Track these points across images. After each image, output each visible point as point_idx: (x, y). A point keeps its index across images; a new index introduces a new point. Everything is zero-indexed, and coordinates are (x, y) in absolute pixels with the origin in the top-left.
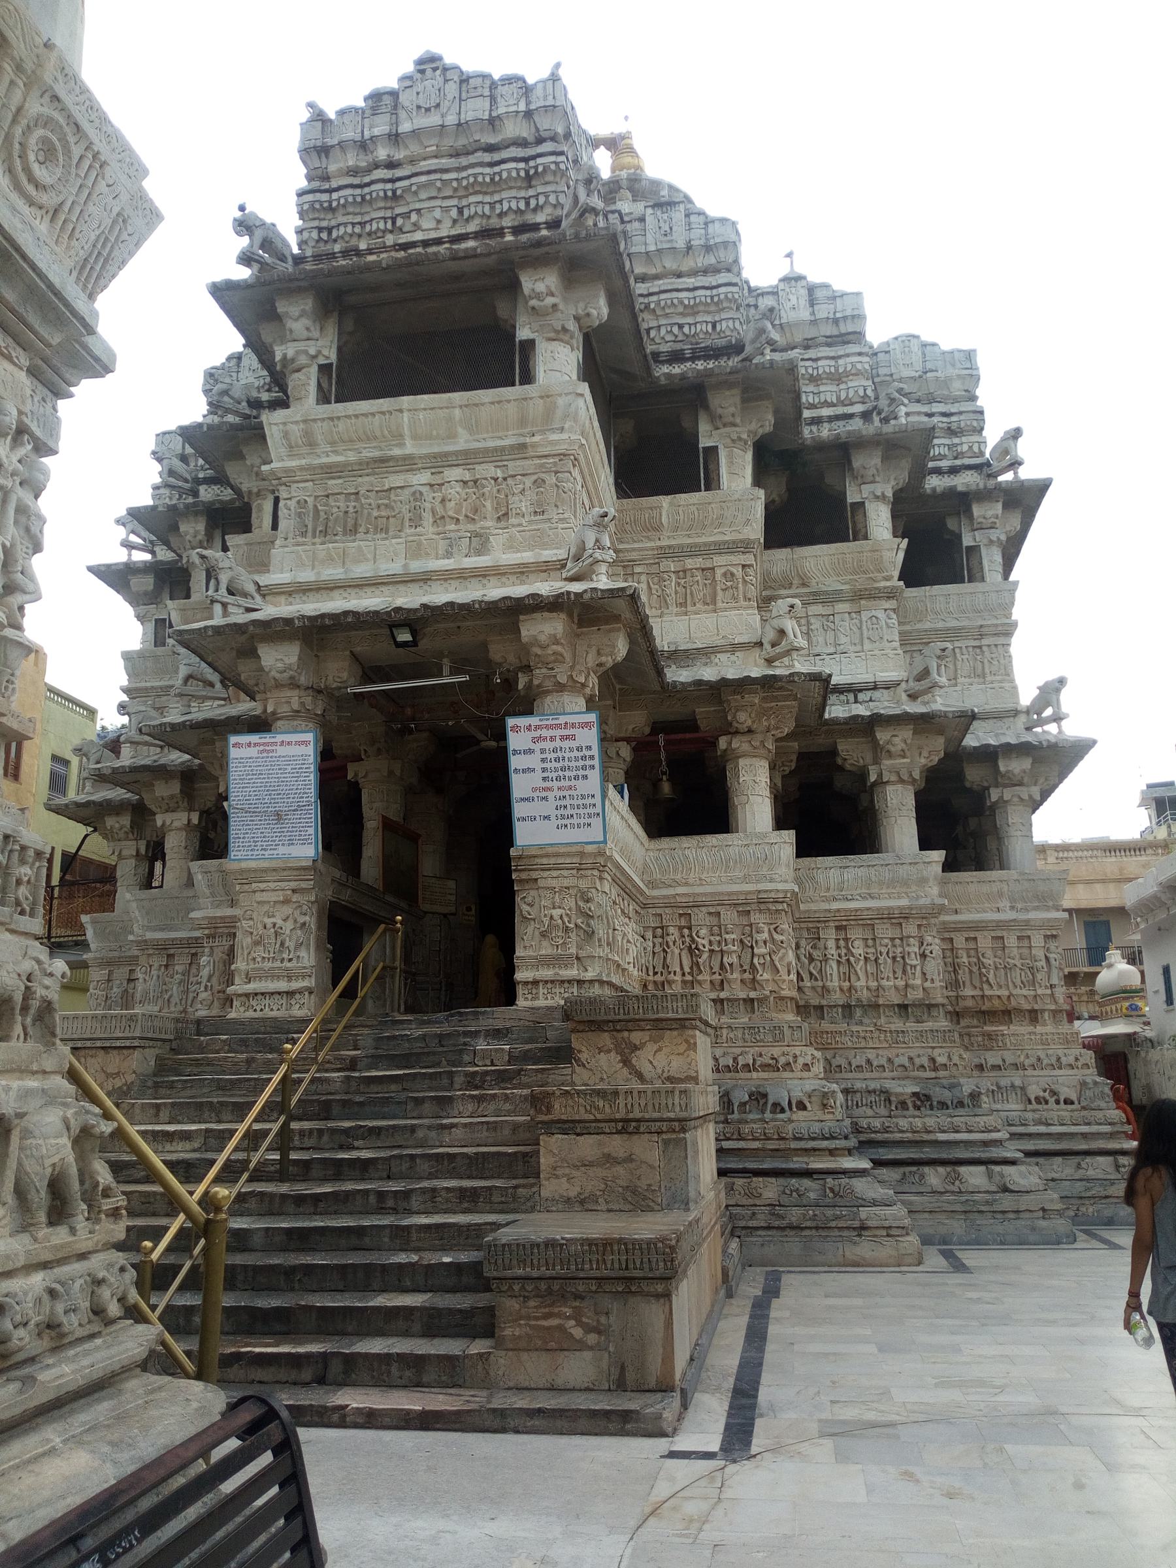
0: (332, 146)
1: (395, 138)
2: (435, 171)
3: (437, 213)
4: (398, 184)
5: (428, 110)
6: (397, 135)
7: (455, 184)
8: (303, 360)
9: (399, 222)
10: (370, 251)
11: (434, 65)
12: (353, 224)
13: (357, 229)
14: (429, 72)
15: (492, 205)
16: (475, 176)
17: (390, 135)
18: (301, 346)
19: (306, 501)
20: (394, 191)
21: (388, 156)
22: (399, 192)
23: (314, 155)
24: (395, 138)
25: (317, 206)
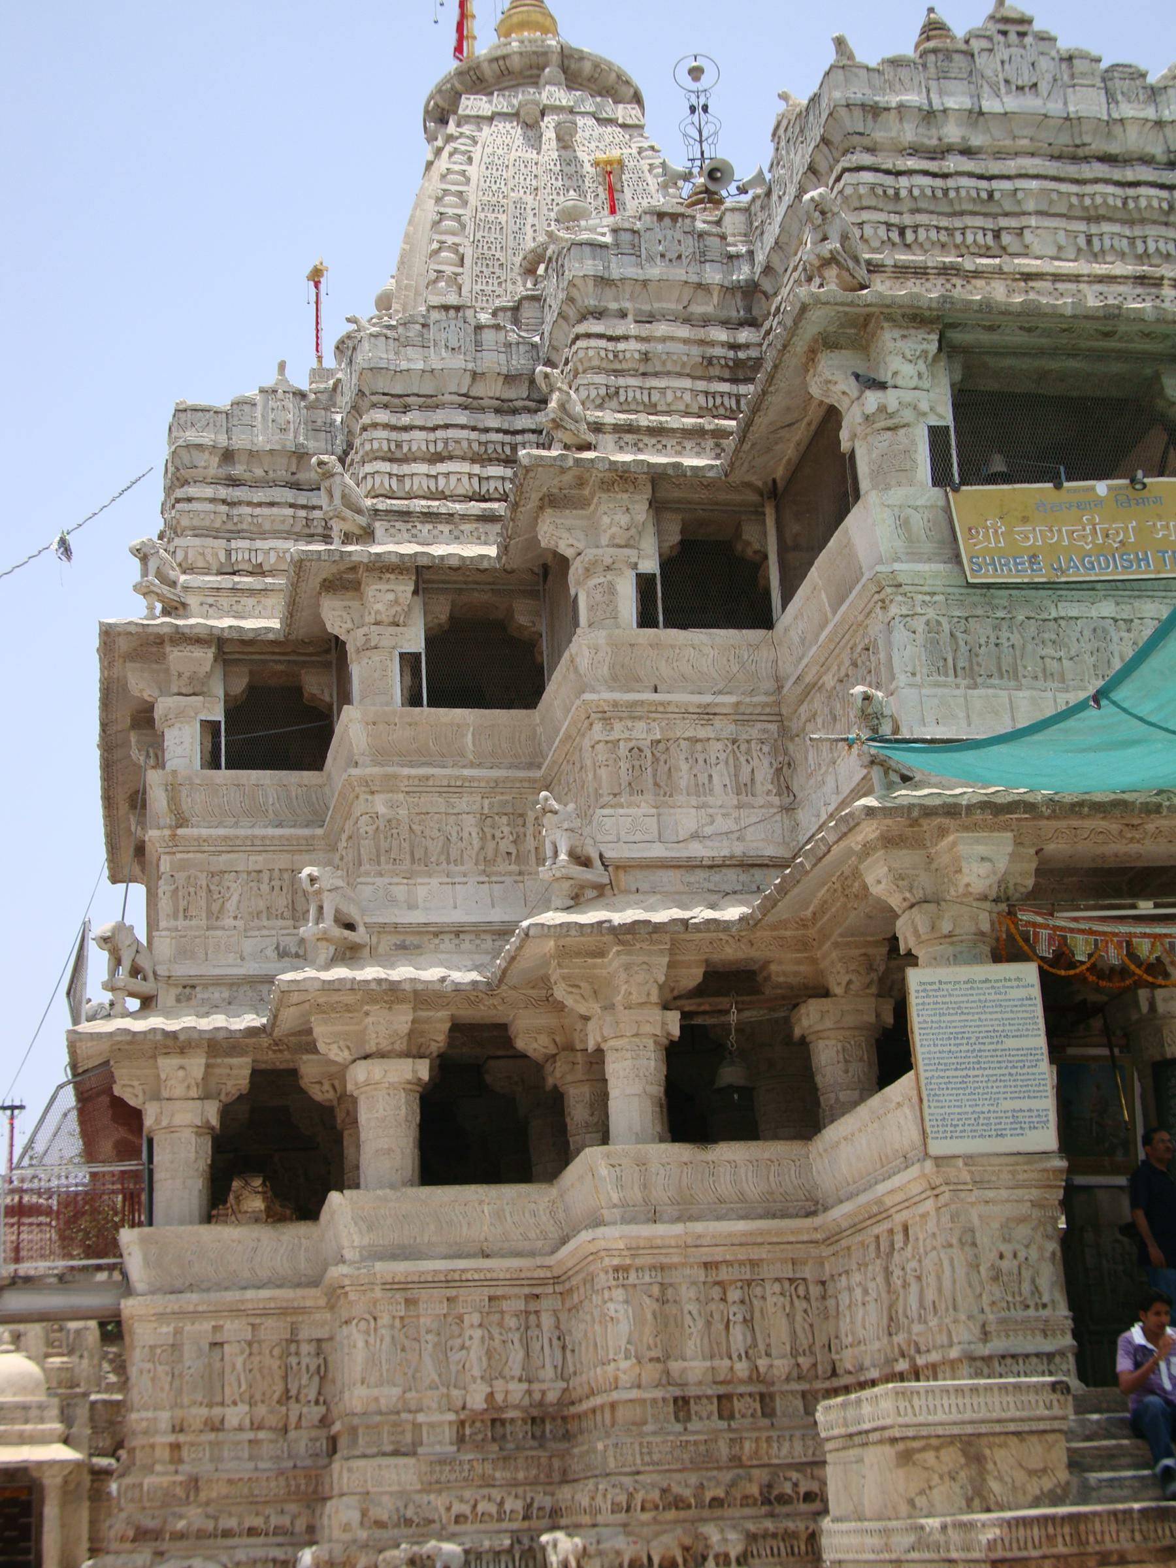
0: (887, 109)
1: (976, 115)
2: (1045, 177)
3: (1061, 238)
4: (995, 184)
5: (1020, 88)
6: (981, 113)
7: (1074, 200)
8: (908, 415)
9: (1006, 239)
10: (977, 274)
11: (1021, 28)
12: (938, 228)
13: (943, 236)
14: (1013, 37)
15: (1132, 240)
16: (1104, 195)
17: (970, 112)
18: (909, 396)
19: (939, 623)
20: (991, 195)
21: (963, 138)
22: (997, 195)
23: (858, 113)
24: (976, 115)
25: (880, 191)
